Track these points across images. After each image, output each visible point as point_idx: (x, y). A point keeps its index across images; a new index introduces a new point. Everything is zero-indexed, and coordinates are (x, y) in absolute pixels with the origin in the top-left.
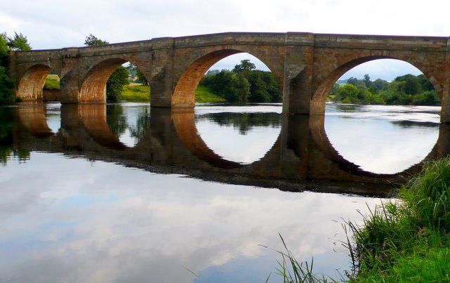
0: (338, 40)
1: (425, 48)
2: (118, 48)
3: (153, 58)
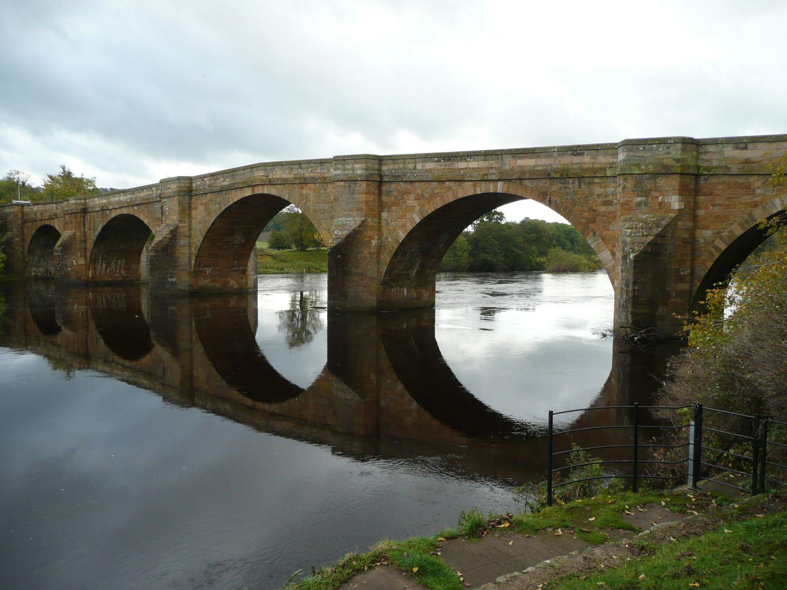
2: (144, 194)
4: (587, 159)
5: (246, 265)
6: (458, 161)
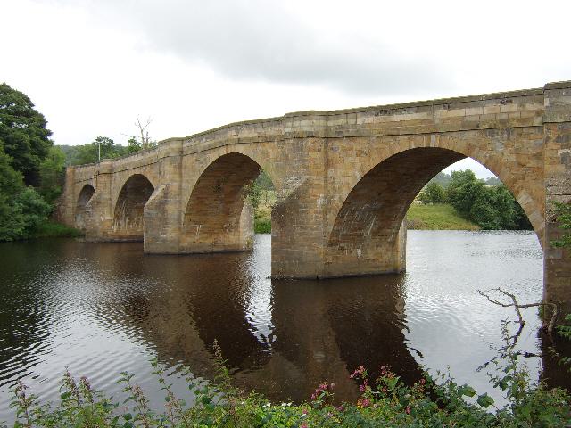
0: (360, 121)
1: (502, 121)
5: (238, 222)
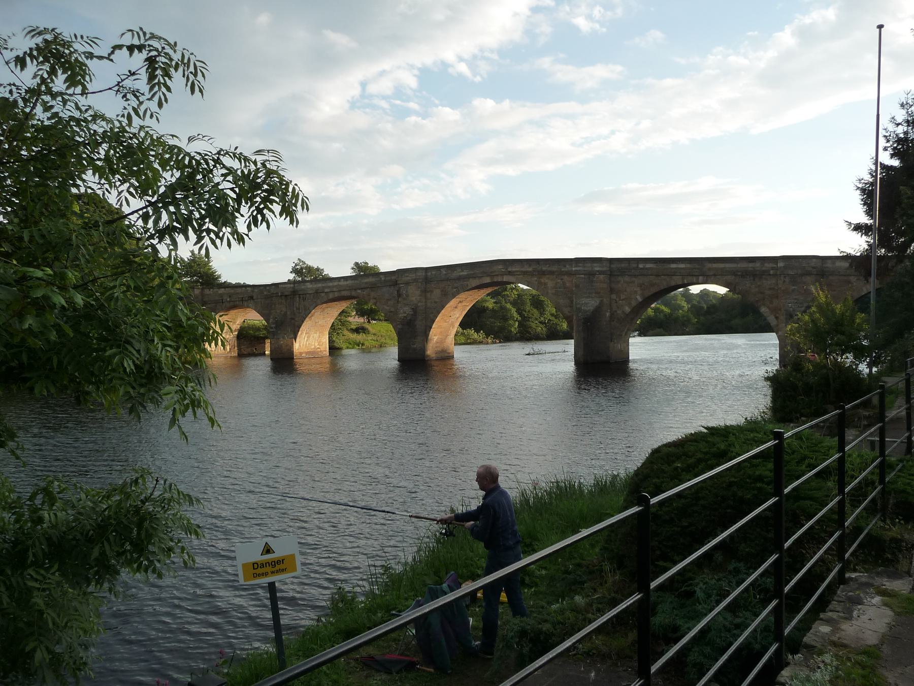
0: (641, 266)
3: (399, 295)
4: (758, 265)
6: (670, 263)
